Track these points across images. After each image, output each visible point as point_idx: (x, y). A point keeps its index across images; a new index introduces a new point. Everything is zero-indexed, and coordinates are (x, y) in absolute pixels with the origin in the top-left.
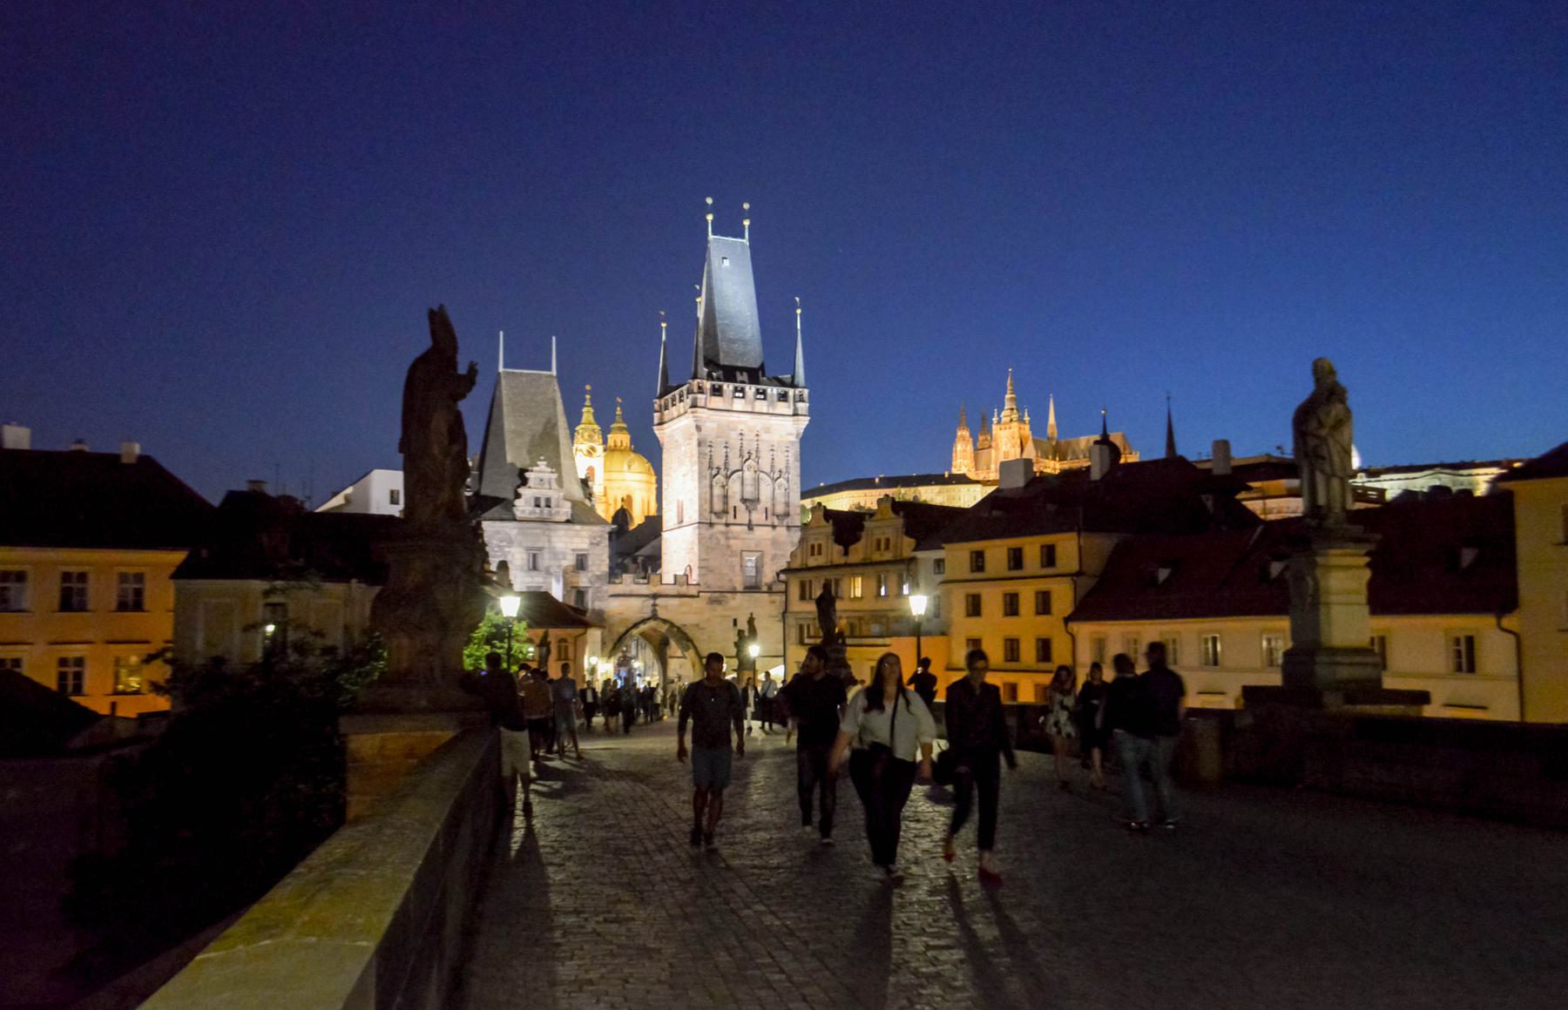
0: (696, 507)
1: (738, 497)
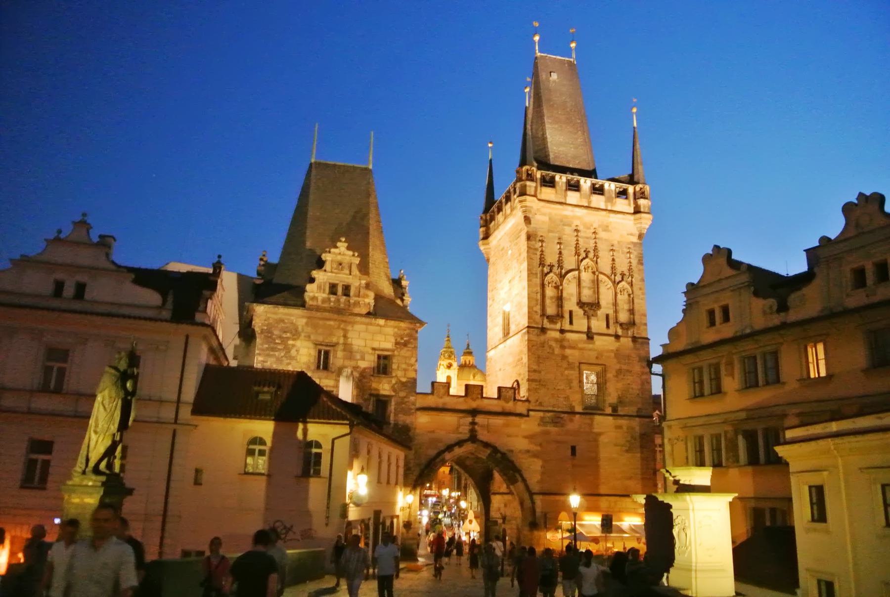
0: (525, 310)
1: (574, 300)
